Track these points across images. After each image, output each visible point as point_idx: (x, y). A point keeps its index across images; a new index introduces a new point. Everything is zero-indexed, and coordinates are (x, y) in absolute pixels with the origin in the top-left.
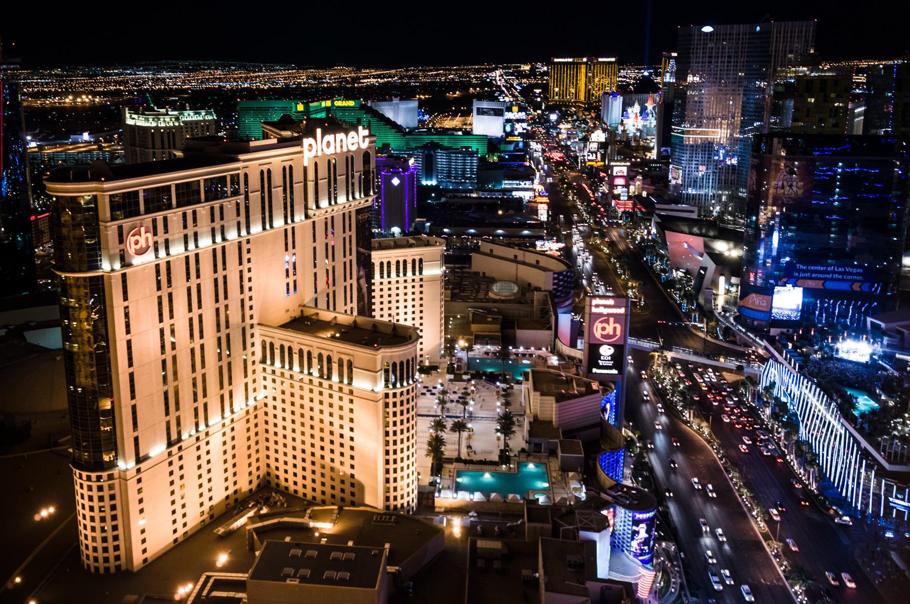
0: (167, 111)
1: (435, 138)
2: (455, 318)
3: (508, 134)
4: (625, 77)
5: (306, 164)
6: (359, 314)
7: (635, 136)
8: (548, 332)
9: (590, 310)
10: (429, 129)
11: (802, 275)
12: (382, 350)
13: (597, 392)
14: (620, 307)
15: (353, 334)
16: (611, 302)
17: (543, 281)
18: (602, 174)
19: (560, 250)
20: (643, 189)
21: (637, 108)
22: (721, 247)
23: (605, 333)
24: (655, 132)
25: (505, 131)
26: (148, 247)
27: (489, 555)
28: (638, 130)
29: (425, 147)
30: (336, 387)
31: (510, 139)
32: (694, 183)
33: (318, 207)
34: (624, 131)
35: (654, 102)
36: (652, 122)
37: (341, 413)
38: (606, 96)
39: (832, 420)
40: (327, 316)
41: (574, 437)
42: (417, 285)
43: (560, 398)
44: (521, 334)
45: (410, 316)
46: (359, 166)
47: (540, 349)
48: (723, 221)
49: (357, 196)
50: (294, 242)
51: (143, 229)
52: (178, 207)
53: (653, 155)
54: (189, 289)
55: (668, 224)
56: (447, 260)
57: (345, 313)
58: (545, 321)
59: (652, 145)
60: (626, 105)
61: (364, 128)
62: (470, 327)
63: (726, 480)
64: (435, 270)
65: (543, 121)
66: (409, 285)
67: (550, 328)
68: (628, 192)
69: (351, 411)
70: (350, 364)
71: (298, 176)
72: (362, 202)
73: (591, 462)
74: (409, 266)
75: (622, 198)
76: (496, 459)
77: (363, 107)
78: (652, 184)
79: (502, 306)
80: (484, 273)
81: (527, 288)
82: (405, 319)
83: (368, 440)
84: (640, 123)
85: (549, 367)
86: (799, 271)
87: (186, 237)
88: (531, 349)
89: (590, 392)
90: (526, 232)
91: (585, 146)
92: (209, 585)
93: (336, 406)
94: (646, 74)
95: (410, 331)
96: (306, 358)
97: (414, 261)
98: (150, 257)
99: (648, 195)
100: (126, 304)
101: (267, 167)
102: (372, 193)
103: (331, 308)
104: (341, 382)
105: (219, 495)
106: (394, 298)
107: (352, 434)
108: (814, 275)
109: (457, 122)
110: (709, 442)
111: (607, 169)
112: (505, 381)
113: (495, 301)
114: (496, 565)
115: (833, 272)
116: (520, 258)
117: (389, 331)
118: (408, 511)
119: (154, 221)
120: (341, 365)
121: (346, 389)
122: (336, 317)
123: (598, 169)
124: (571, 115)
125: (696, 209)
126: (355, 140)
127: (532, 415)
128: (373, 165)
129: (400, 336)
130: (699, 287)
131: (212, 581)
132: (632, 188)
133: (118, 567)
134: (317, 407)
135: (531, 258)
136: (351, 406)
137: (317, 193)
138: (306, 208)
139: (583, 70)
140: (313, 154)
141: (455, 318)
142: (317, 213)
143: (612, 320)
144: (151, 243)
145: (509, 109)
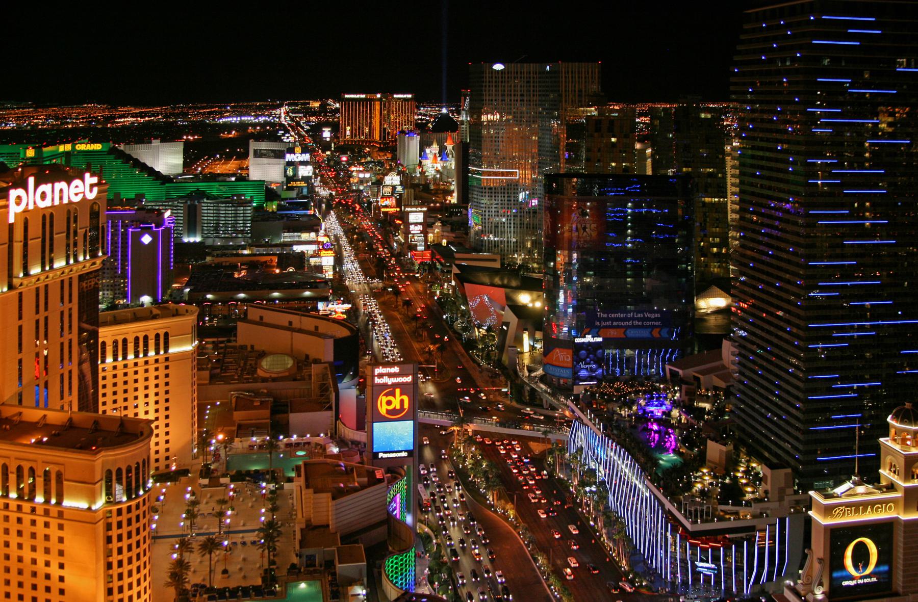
1: (202, 186)
2: (213, 405)
3: (289, 179)
4: (425, 115)
6: (80, 409)
7: (434, 178)
9: (373, 380)
10: (196, 175)
11: (603, 324)
12: (103, 453)
13: (381, 481)
15: (66, 437)
16: (396, 370)
19: (347, 312)
20: (443, 237)
21: (435, 148)
22: (524, 298)
24: (454, 173)
25: (286, 175)
28: (438, 171)
29: (190, 196)
30: (40, 510)
31: (293, 184)
32: (496, 229)
33: (26, 274)
34: (423, 173)
35: (452, 139)
36: (452, 164)
37: (47, 544)
38: (402, 135)
39: (637, 483)
40: (33, 415)
41: (356, 542)
42: (161, 366)
43: (338, 494)
44: (295, 418)
45: (152, 407)
47: (319, 436)
48: (527, 269)
49: (81, 258)
53: (453, 199)
55: (466, 276)
56: (201, 332)
57: (61, 409)
58: (325, 399)
59: (452, 188)
60: (424, 145)
62: (232, 415)
63: (534, 570)
65: (333, 163)
66: (151, 368)
67: (330, 408)
68: (426, 240)
69: (61, 540)
70: (59, 476)
72: (88, 265)
73: (376, 570)
75: (419, 248)
77: (113, 151)
78: (452, 230)
80: (252, 347)
81: (303, 362)
82: (144, 409)
84: (439, 166)
85: (327, 456)
86: (600, 320)
88: (307, 433)
89: (374, 481)
90: (307, 293)
91: (379, 191)
93: (40, 536)
94: (444, 111)
95: (142, 425)
97: (157, 336)
99: (448, 243)
102: (100, 254)
103: (42, 404)
104: (47, 501)
106: (131, 386)
108: (615, 324)
109: (232, 166)
110: (516, 528)
111: (404, 217)
112: (274, 479)
113: (264, 380)
115: (633, 319)
116: (296, 325)
117: (115, 428)
120: (47, 481)
121: (54, 511)
122: (45, 416)
123: (394, 216)
125: (498, 257)
127: (304, 520)
129: (131, 432)
130: (501, 347)
132: (431, 236)
136: (61, 533)
137: (25, 256)
138: (10, 276)
141: (213, 405)
143: (398, 391)
145: (291, 151)
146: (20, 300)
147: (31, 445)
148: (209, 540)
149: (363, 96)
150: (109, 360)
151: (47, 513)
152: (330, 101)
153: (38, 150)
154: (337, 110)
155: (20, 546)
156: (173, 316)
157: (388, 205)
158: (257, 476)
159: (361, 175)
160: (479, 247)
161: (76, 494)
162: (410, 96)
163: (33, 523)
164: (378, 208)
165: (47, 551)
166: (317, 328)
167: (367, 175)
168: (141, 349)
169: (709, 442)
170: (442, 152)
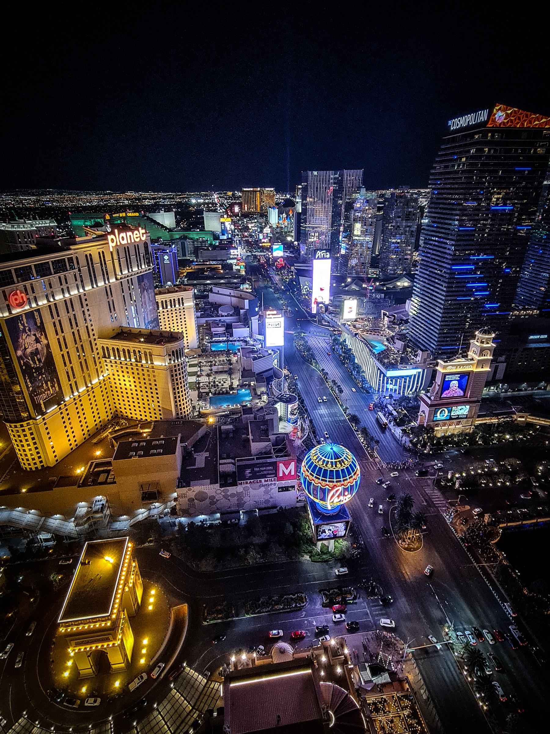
0: (25, 221)
5: (111, 250)
13: (271, 354)
27: (227, 432)
46: (142, 250)
49: (143, 267)
51: (18, 291)
56: (196, 297)
60: (280, 213)
61: (142, 229)
67: (249, 327)
71: (108, 258)
74: (177, 302)
92: (93, 466)
101: (89, 252)
105: (91, 425)
114: (231, 435)
120: (146, 355)
126: (138, 235)
128: (150, 249)
131: (94, 464)
133: (43, 466)
138: (116, 275)
140: (114, 244)
149: (252, 189)
152: (236, 192)
153: (111, 215)
154: (240, 197)
156: (184, 291)
162: (272, 189)
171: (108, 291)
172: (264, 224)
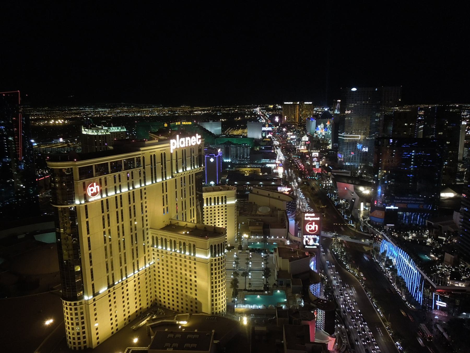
1: (230, 139)
2: (241, 224)
7: (322, 138)
8: (285, 229)
11: (397, 201)
12: (210, 239)
13: (307, 256)
14: (318, 217)
16: (313, 215)
17: (283, 206)
18: (307, 156)
20: (326, 163)
21: (322, 125)
22: (361, 189)
23: (311, 229)
24: (331, 137)
25: (262, 136)
26: (97, 192)
29: (225, 143)
31: (265, 139)
32: (349, 160)
33: (178, 172)
37: (190, 269)
40: (183, 224)
42: (224, 208)
44: (272, 230)
45: (221, 223)
49: (196, 167)
50: (166, 189)
51: (95, 184)
52: (111, 173)
53: (330, 147)
54: (117, 212)
56: (237, 197)
57: (192, 221)
58: (284, 224)
64: (232, 202)
65: (280, 131)
67: (285, 228)
68: (319, 164)
69: (195, 268)
70: (194, 246)
72: (198, 169)
74: (220, 200)
76: (262, 289)
78: (330, 161)
79: (263, 217)
80: (254, 203)
81: (274, 209)
82: (220, 224)
83: (203, 281)
87: (115, 187)
90: (273, 183)
91: (299, 143)
93: (188, 266)
96: (174, 244)
98: (98, 197)
100: (87, 220)
103: (184, 220)
104: (190, 254)
107: (196, 279)
108: (403, 202)
109: (239, 132)
111: (310, 153)
112: (265, 253)
113: (260, 216)
115: (411, 200)
118: (222, 315)
119: (100, 179)
123: (306, 154)
124: (292, 128)
125: (350, 172)
129: (217, 232)
134: (179, 267)
135: (276, 195)
136: (195, 266)
137: (177, 165)
138: (172, 173)
139: (298, 108)
141: (241, 224)
142: (177, 175)
143: (314, 223)
144: (99, 190)
145: (264, 126)
146: (176, 182)
147: (183, 234)
148: (244, 273)
150: (205, 205)
151: (190, 258)
155: (181, 269)
157: (303, 149)
158: (259, 251)
159: (292, 137)
160: (342, 167)
161: (201, 252)
163: (185, 261)
164: (299, 150)
165: (190, 271)
166: (279, 197)
167: (294, 137)
168: (216, 202)
169: (446, 253)
170: (325, 127)
171: (164, 186)
172: (301, 133)
